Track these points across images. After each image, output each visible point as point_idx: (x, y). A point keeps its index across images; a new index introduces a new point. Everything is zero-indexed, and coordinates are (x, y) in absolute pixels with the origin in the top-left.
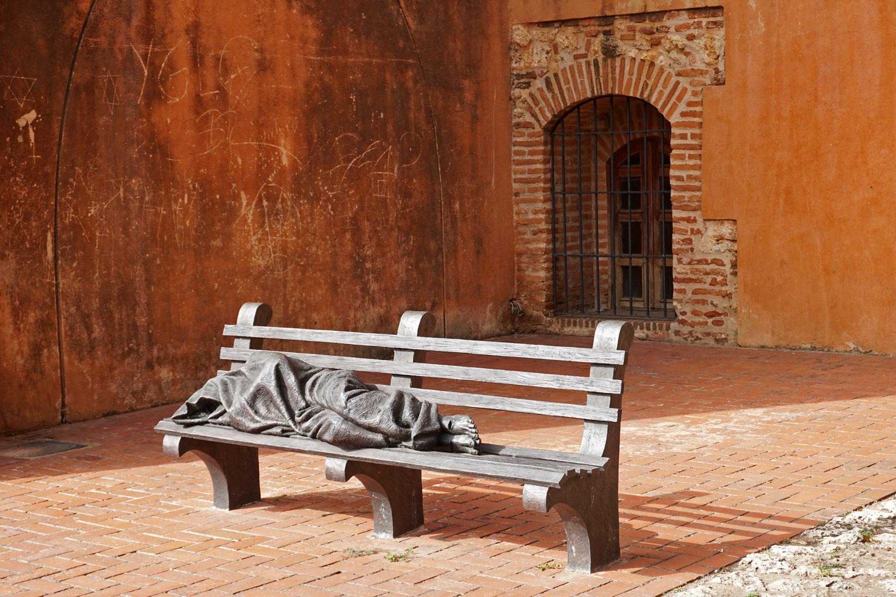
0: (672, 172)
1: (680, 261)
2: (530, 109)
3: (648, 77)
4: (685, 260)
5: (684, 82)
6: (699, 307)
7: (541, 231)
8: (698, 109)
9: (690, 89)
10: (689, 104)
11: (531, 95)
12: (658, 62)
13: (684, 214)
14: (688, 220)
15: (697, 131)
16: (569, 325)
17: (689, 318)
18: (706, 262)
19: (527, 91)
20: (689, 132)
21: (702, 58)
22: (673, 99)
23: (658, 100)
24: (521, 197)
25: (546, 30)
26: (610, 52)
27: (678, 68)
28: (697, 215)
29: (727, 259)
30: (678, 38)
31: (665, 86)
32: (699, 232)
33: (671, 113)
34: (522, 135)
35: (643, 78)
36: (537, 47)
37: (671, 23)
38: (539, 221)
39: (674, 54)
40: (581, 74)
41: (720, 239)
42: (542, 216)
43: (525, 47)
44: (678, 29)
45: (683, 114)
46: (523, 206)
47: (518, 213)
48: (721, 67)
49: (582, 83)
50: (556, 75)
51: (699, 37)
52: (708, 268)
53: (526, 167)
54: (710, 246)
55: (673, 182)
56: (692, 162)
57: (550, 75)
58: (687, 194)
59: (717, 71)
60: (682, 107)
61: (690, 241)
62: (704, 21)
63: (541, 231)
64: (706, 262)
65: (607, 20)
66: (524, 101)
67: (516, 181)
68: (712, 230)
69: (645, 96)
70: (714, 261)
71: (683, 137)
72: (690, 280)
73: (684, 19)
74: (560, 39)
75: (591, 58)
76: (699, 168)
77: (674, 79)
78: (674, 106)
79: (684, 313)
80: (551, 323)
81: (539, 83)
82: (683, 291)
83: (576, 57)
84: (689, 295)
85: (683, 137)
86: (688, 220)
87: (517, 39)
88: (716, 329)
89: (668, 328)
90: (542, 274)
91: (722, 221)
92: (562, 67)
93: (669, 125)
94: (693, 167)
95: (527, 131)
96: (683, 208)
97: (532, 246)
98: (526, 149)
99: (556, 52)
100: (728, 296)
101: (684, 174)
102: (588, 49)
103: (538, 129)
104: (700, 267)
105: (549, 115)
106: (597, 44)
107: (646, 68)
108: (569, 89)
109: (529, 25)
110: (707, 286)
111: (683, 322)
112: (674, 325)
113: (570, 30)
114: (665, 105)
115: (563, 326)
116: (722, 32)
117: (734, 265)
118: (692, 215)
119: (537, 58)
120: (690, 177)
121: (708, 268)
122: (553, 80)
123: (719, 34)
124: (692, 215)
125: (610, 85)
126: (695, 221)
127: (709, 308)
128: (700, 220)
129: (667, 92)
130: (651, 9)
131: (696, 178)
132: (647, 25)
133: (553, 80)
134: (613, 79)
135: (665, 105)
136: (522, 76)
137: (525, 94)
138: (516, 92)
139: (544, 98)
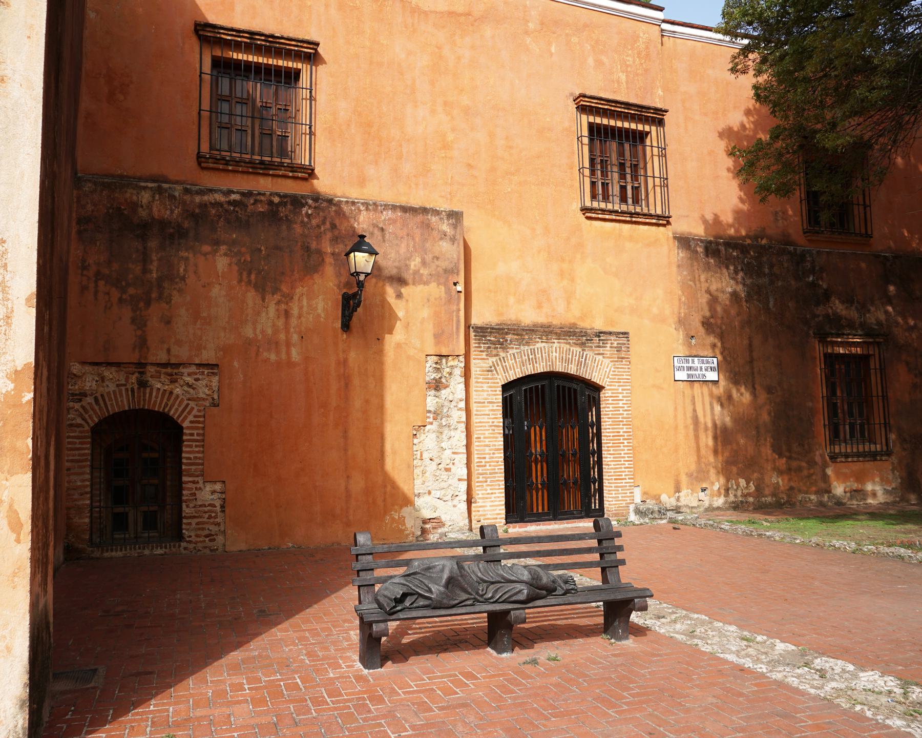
0: (184, 455)
1: (187, 506)
2: (81, 415)
3: (168, 399)
4: (191, 505)
5: (192, 404)
6: (199, 532)
7: (86, 493)
8: (201, 419)
9: (196, 408)
10: (195, 416)
11: (83, 407)
12: (175, 392)
13: (191, 479)
14: (194, 482)
15: (201, 432)
16: (107, 551)
17: (193, 539)
18: (205, 506)
19: (80, 404)
20: (195, 432)
21: (203, 392)
22: (185, 413)
23: (174, 414)
24: (72, 471)
25: (96, 368)
26: (143, 384)
27: (188, 396)
28: (200, 479)
29: (218, 504)
30: (189, 379)
31: (179, 406)
32: (200, 489)
33: (183, 421)
34: (76, 431)
35: (165, 400)
36: (89, 378)
37: (185, 371)
38: (86, 486)
39: (186, 388)
40: (121, 395)
41: (213, 492)
42: (88, 483)
43: (80, 377)
44: (189, 375)
45: (191, 422)
46: (73, 478)
47: (69, 482)
48: (216, 397)
49: (122, 401)
50: (102, 396)
51: (202, 380)
52: (206, 509)
53: (77, 452)
54: (207, 496)
55: (184, 461)
56: (197, 449)
57: (98, 395)
58: (193, 467)
59: (213, 399)
60: (191, 418)
61: (195, 494)
62: (206, 372)
63: (86, 493)
64: (205, 506)
65: (141, 366)
66: (77, 410)
67: (67, 461)
68: (208, 488)
69: (166, 410)
70: (210, 505)
71: (192, 435)
72: (195, 517)
73: (193, 369)
74: (107, 374)
75: (129, 387)
76: (203, 452)
77: (186, 402)
78: (186, 418)
79: (190, 536)
80: (93, 552)
81: (90, 400)
82: (190, 524)
83: (118, 386)
84: (194, 525)
85: (192, 435)
86: (194, 482)
87: (75, 371)
88: (211, 544)
89: (180, 546)
90: (87, 520)
91: (215, 482)
92: (107, 390)
93: (182, 428)
94: (198, 452)
95: (78, 429)
96: (190, 476)
97: (80, 503)
98: (77, 441)
99: (103, 381)
100: (218, 524)
101: (192, 456)
102: (127, 379)
103: (87, 428)
104: (201, 509)
105: (96, 420)
106: (133, 379)
107: (167, 395)
108: (112, 405)
109: (83, 363)
110: (205, 520)
111: (190, 542)
112: (183, 544)
113: (113, 369)
114: (179, 416)
115: (102, 552)
116: (217, 378)
117: (222, 507)
118: (196, 479)
119: (89, 383)
120: (196, 458)
121: (206, 509)
122: (100, 398)
123: (215, 380)
124: (196, 479)
125: (142, 403)
126: (198, 482)
127: (207, 532)
128: (201, 482)
129: (180, 409)
130: (172, 361)
131: (200, 458)
132: (169, 370)
133: (100, 398)
134: (144, 400)
135: (179, 416)
136: (76, 395)
137: (77, 406)
138: (71, 404)
139: (93, 409)
